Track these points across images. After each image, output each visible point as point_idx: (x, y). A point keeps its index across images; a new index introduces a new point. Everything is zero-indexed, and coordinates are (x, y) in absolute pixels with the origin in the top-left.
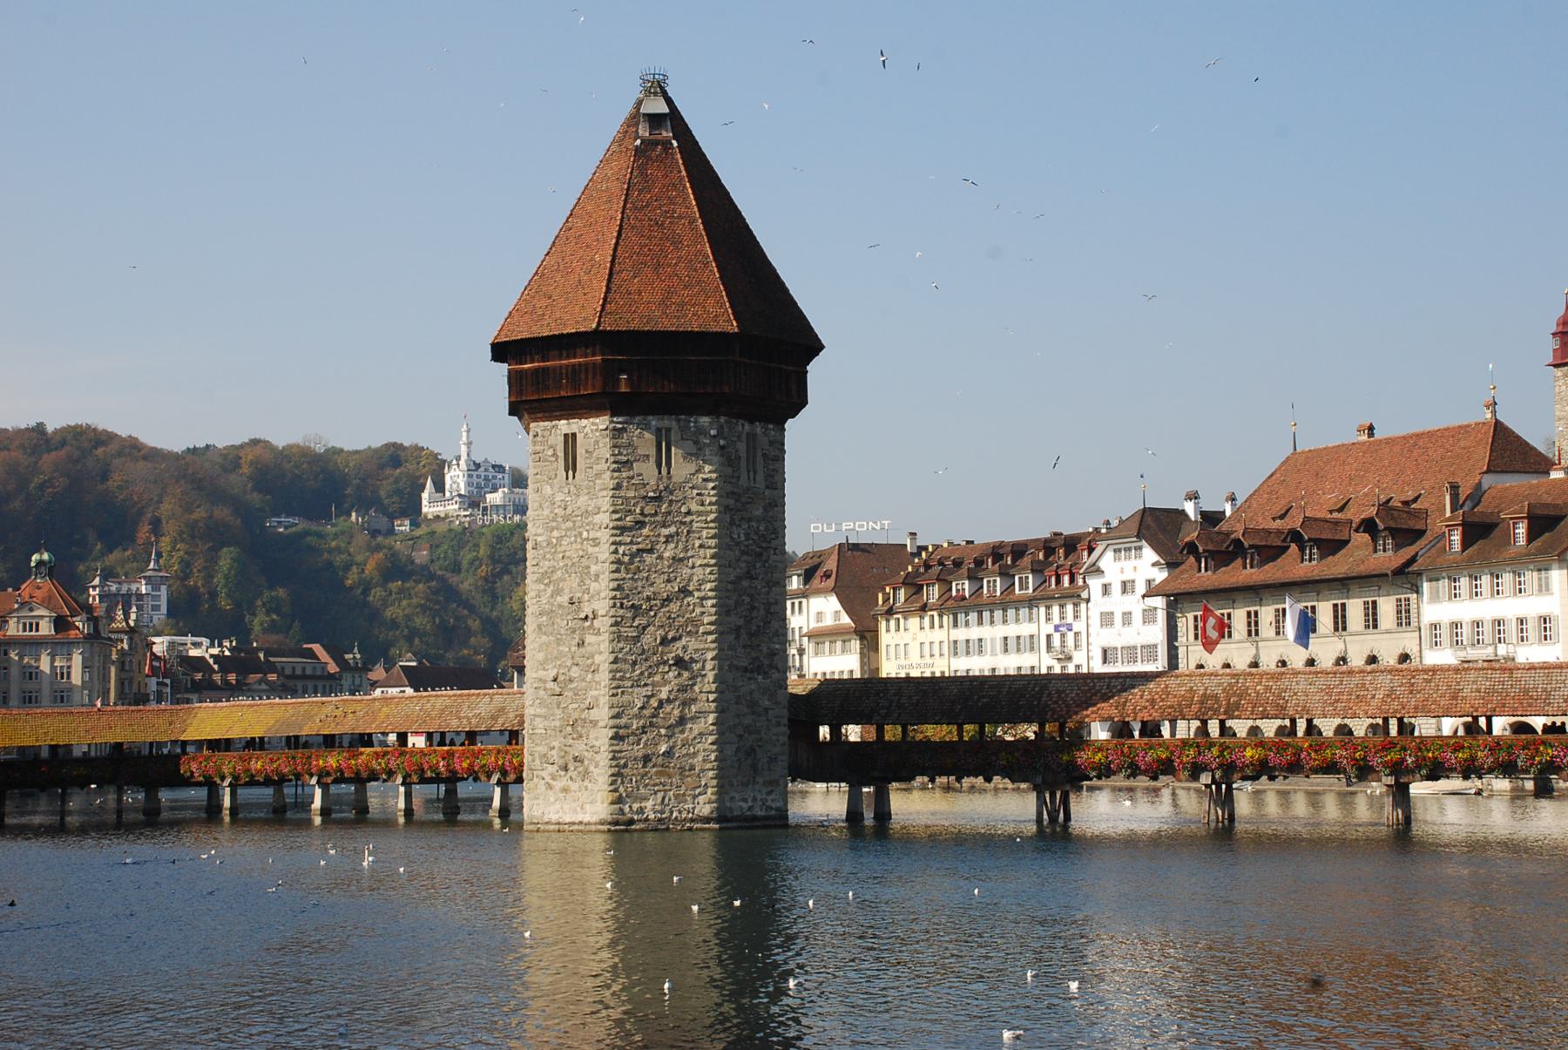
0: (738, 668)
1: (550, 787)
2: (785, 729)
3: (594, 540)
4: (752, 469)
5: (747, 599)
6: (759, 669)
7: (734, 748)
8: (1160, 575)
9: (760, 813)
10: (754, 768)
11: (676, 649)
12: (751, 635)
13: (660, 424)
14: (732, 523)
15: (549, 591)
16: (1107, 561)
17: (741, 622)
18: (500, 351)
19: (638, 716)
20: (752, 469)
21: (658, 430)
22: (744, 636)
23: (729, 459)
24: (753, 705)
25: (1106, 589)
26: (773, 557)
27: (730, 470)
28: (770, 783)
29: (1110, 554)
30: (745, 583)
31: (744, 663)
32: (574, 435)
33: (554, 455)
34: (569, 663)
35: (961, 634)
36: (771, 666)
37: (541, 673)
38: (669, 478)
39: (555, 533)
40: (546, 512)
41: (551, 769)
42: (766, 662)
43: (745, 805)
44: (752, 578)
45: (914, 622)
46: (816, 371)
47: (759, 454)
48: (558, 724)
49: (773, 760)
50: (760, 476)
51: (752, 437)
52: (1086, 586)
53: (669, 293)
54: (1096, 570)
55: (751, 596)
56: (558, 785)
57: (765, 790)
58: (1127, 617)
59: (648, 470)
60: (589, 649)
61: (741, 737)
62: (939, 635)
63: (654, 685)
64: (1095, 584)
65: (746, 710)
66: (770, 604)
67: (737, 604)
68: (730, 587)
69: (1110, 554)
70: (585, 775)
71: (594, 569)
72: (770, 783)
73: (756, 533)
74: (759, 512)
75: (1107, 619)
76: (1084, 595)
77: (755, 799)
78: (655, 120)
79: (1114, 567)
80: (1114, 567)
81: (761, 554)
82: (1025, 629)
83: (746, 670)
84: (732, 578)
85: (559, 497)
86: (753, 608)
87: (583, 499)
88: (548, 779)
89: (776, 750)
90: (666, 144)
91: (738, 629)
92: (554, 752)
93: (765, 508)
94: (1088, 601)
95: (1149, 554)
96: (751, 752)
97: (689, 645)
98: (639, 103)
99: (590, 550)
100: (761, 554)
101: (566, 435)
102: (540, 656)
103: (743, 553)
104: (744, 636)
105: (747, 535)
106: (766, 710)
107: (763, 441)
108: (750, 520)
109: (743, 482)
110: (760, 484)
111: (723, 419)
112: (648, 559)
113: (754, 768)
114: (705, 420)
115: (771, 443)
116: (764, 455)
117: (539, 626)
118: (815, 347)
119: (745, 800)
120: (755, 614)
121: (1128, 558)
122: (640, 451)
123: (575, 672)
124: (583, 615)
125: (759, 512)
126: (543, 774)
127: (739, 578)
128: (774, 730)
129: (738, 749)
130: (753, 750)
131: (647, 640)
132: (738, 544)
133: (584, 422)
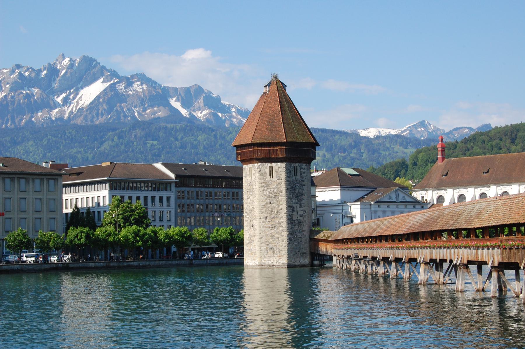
4: (271, 174)
5: (270, 209)
6: (275, 227)
9: (275, 264)
11: (253, 223)
14: (264, 190)
20: (271, 174)
23: (262, 174)
26: (280, 198)
27: (262, 177)
28: (280, 256)
31: (270, 226)
55: (272, 208)
59: (248, 178)
67: (266, 211)
72: (280, 256)
83: (269, 227)
93: (277, 185)
104: (268, 219)
105: (269, 193)
111: (259, 164)
113: (274, 253)
114: (256, 164)
116: (276, 171)
125: (275, 186)
129: (267, 248)
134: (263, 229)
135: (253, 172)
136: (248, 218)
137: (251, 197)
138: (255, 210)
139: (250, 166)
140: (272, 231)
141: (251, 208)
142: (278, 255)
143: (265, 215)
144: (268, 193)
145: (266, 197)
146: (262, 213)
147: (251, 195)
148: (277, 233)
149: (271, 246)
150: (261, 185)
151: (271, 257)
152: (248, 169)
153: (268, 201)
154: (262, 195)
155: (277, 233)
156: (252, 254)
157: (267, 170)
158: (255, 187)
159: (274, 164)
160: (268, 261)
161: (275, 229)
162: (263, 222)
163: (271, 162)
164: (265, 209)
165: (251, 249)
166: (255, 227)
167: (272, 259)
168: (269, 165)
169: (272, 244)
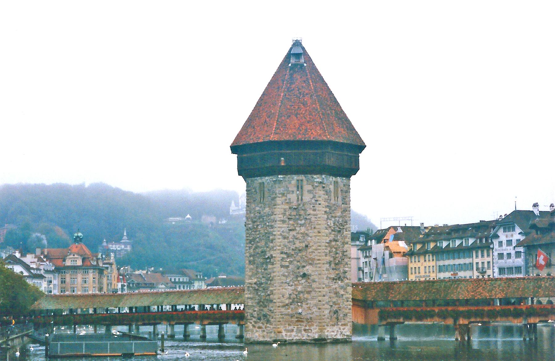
0: (330, 278)
1: (254, 326)
2: (351, 304)
3: (271, 226)
4: (336, 196)
5: (334, 250)
6: (339, 278)
7: (328, 311)
8: (522, 238)
9: (339, 337)
10: (337, 319)
11: (305, 270)
12: (336, 264)
13: (298, 178)
14: (327, 219)
15: (253, 247)
16: (501, 233)
17: (332, 259)
18: (234, 149)
19: (290, 298)
21: (298, 180)
22: (333, 265)
23: (326, 191)
24: (336, 293)
25: (501, 243)
27: (327, 196)
29: (501, 230)
30: (333, 243)
31: (333, 276)
32: (263, 183)
33: (255, 191)
34: (261, 276)
35: (441, 263)
36: (344, 277)
37: (250, 281)
38: (302, 200)
39: (256, 224)
40: (252, 215)
41: (254, 319)
42: (342, 276)
43: (332, 333)
44: (336, 241)
45: (422, 259)
46: (363, 157)
47: (339, 190)
48: (257, 301)
49: (345, 315)
50: (340, 199)
51: (336, 183)
52: (492, 243)
53: (301, 125)
54: (497, 237)
56: (257, 325)
57: (342, 328)
58: (509, 255)
60: (269, 271)
61: (331, 306)
62: (432, 263)
63: (295, 285)
64: (496, 242)
65: (334, 296)
66: (344, 252)
67: (330, 252)
68: (327, 244)
69: (501, 230)
70: (268, 321)
71: (271, 237)
73: (338, 222)
74: (339, 214)
75: (501, 256)
76: (492, 246)
77: (338, 331)
78: (298, 56)
79: (503, 236)
80: (503, 236)
81: (339, 231)
82: (467, 261)
83: (334, 279)
84: (328, 241)
85: (257, 209)
86: (337, 253)
87: (267, 209)
88: (253, 323)
89: (347, 311)
90: (302, 65)
91: (330, 263)
92: (255, 313)
94: (493, 249)
95: (518, 230)
96: (336, 312)
97: (309, 269)
98: (291, 49)
99: (270, 230)
100: (339, 231)
101: (260, 183)
102: (250, 274)
103: (332, 230)
105: (334, 223)
106: (342, 295)
107: (341, 185)
108: (336, 217)
109: (333, 201)
110: (340, 202)
111: (323, 176)
112: (292, 233)
113: (337, 319)
115: (344, 185)
116: (341, 190)
117: (250, 262)
118: (361, 147)
119: (333, 332)
120: (337, 255)
121: (509, 231)
122: (290, 189)
123: (263, 281)
124: (267, 257)
126: (251, 321)
127: (331, 241)
128: (346, 303)
130: (337, 311)
131: (291, 267)
132: (330, 227)
133: (267, 178)
134: (326, 282)
135: (307, 187)
136: (291, 262)
137: (303, 229)
138: (310, 250)
139: (296, 177)
140: (336, 286)
141: (298, 245)
142: (343, 323)
143: (328, 258)
144: (332, 224)
145: (330, 231)
146: (326, 255)
147: (301, 225)
148: (342, 288)
149: (335, 308)
150: (325, 209)
151: (333, 325)
152: (294, 182)
153: (332, 237)
154: (326, 226)
155: (342, 288)
156: (298, 321)
157: (332, 187)
158: (312, 212)
159: (339, 179)
160: (332, 332)
161: (340, 282)
162: (327, 270)
163: (336, 175)
164: (329, 249)
165: (300, 313)
166: (312, 278)
167: (335, 328)
168: (334, 179)
169: (335, 304)
